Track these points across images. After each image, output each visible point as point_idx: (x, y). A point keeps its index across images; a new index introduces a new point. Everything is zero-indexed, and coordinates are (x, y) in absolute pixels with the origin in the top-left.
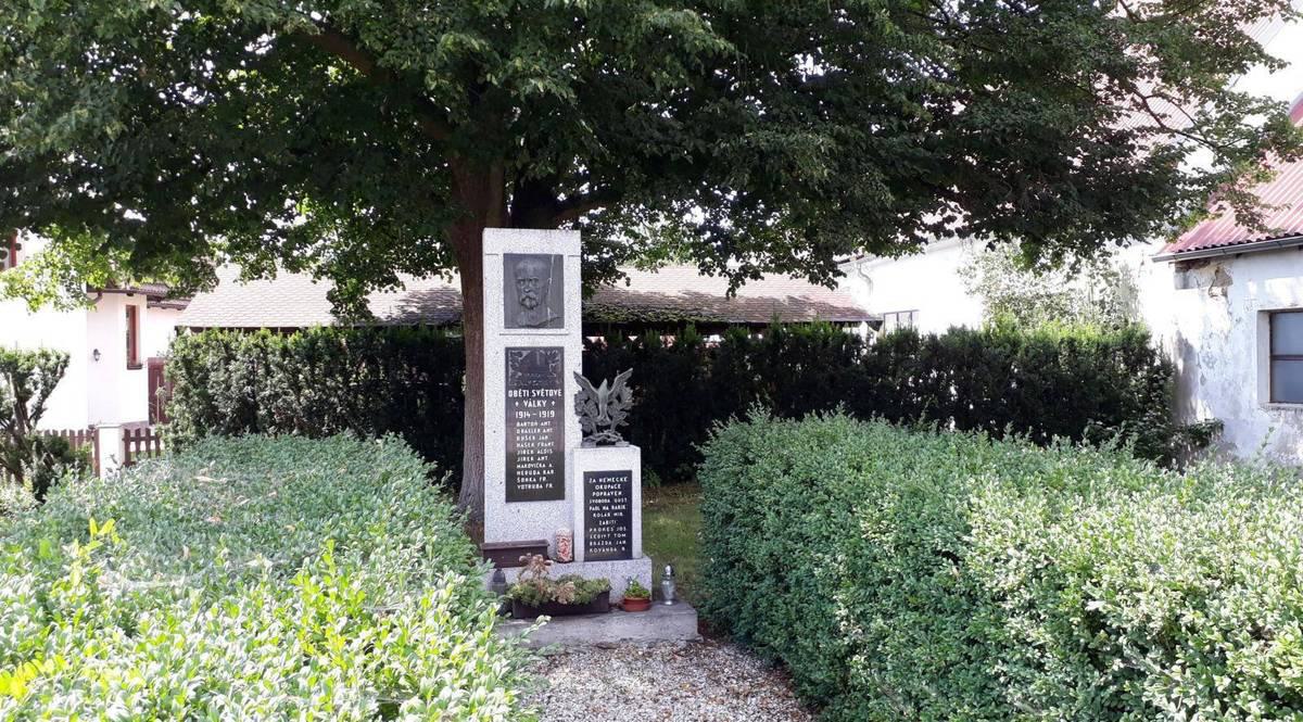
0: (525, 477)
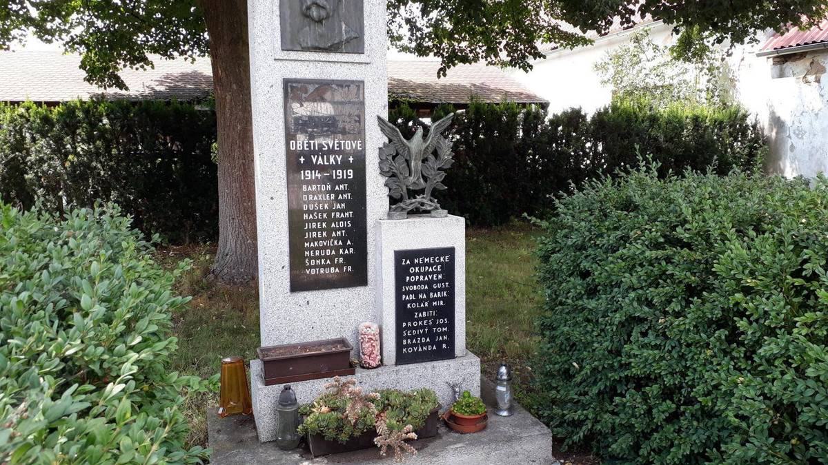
0: (316, 258)
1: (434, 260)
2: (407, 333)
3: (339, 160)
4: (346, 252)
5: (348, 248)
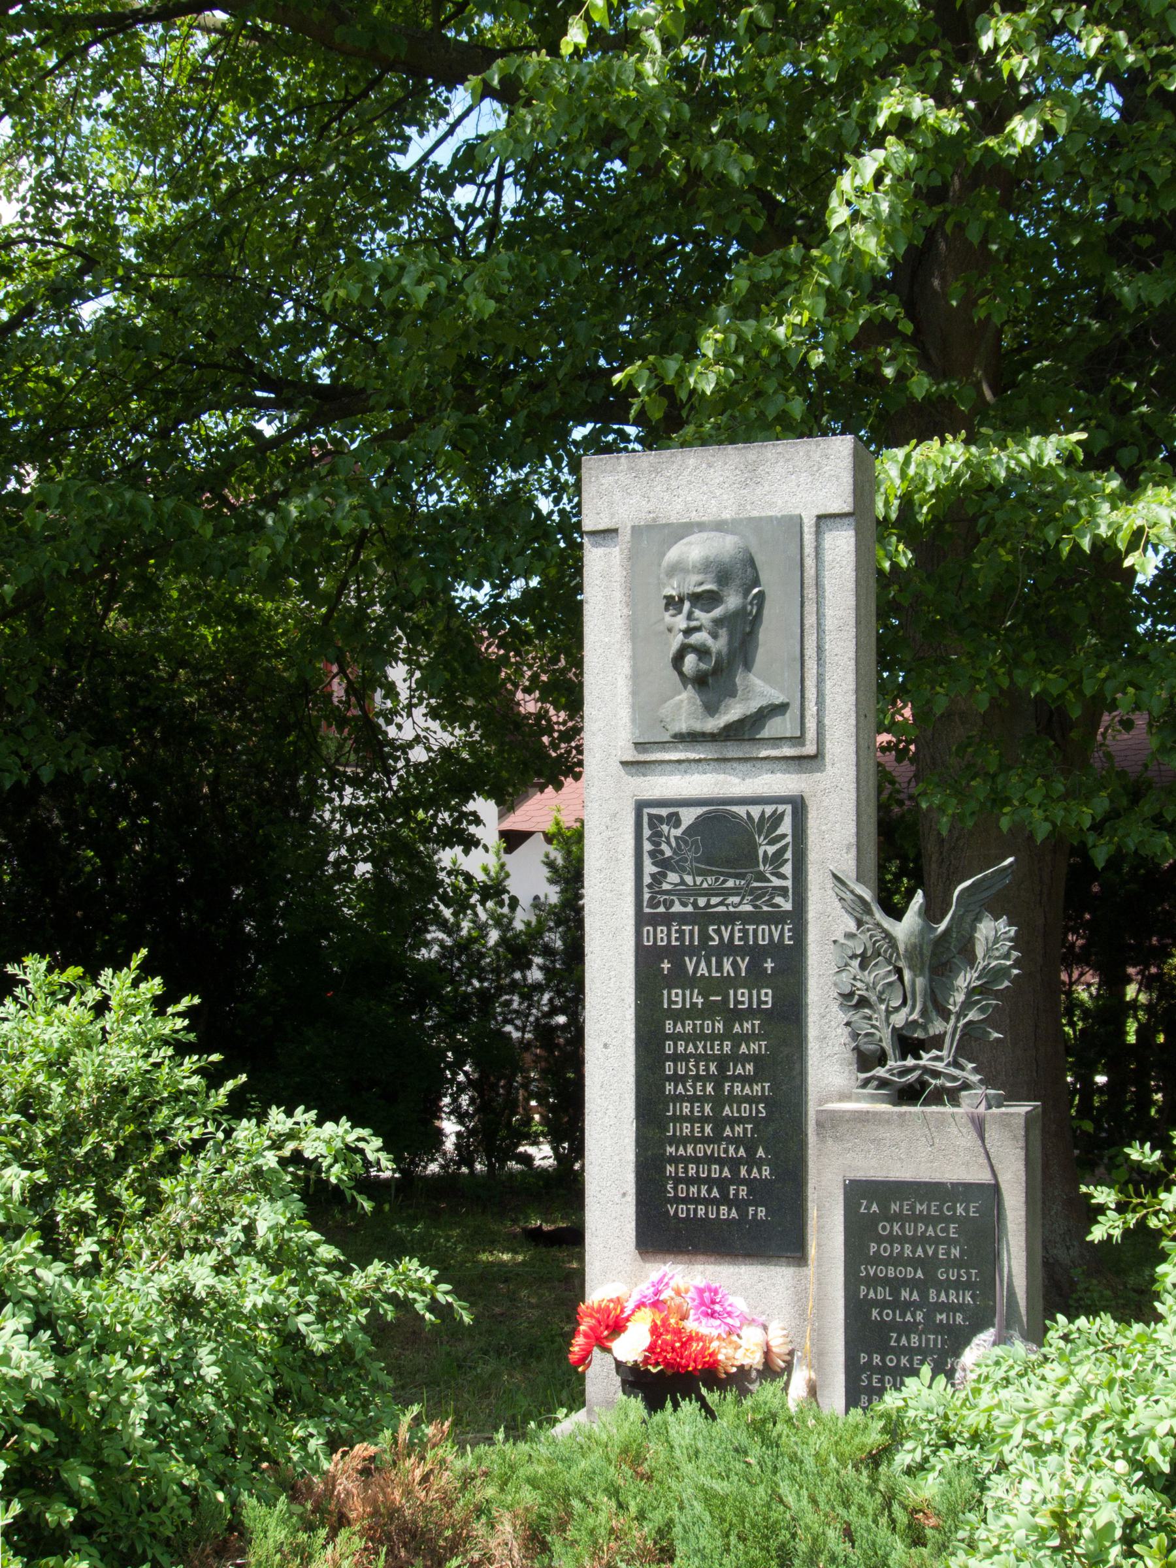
0: (689, 1181)
1: (939, 1209)
2: (869, 1378)
3: (743, 966)
4: (755, 1173)
5: (759, 1163)
